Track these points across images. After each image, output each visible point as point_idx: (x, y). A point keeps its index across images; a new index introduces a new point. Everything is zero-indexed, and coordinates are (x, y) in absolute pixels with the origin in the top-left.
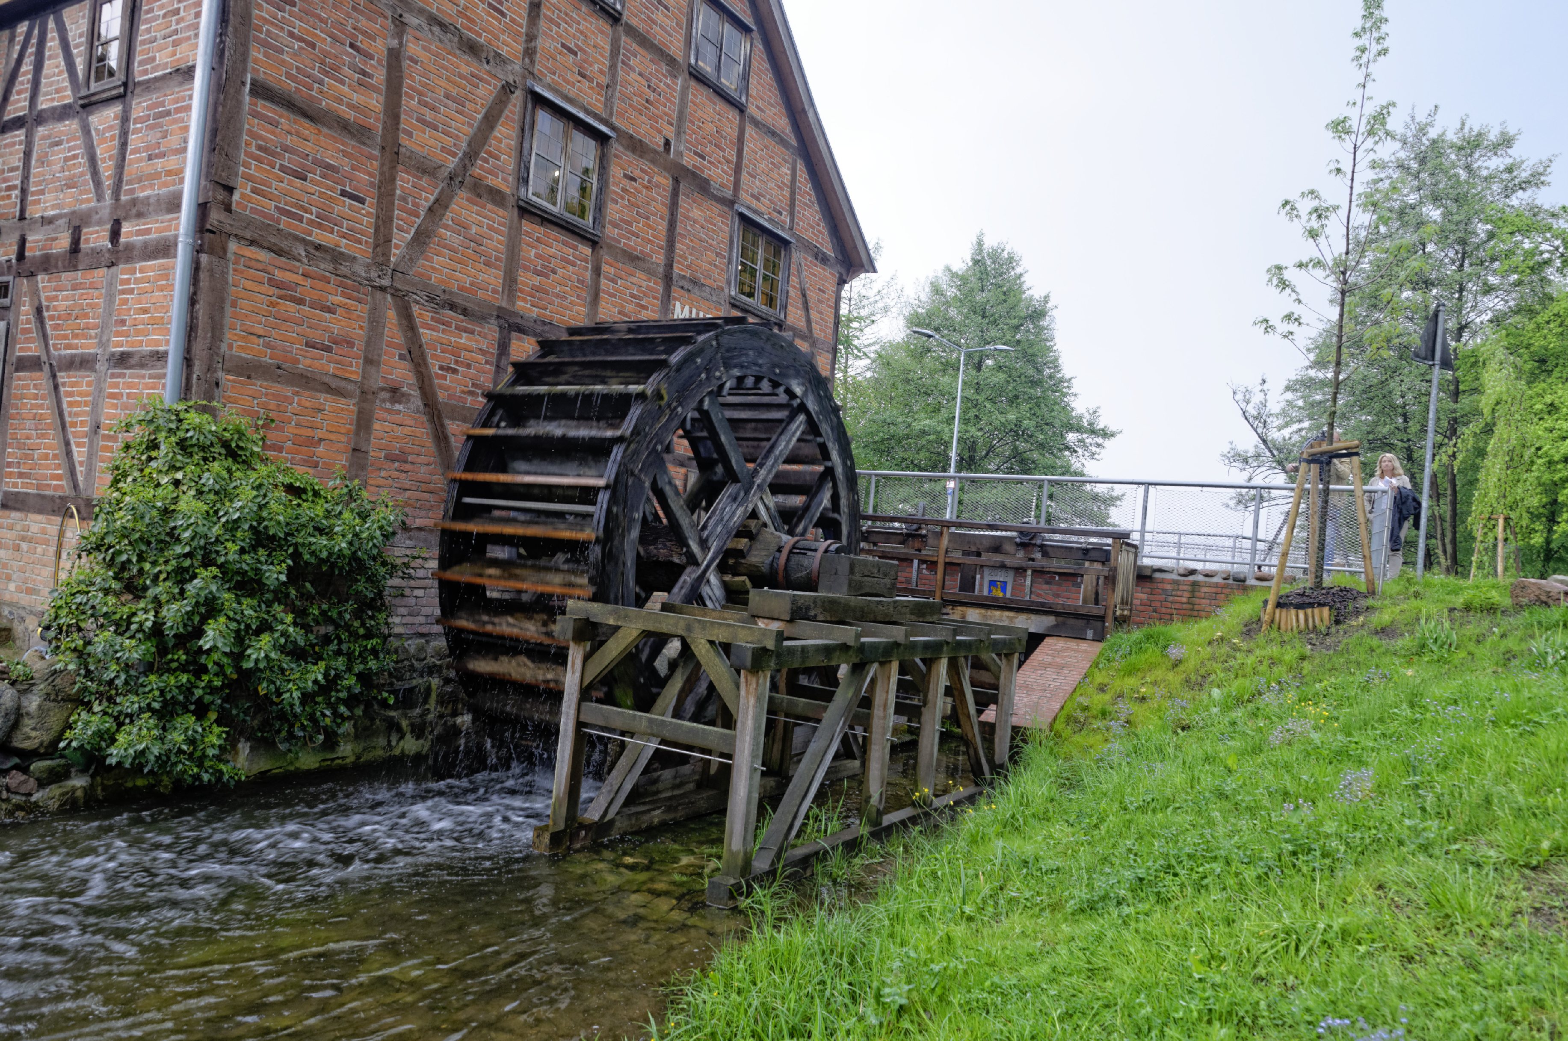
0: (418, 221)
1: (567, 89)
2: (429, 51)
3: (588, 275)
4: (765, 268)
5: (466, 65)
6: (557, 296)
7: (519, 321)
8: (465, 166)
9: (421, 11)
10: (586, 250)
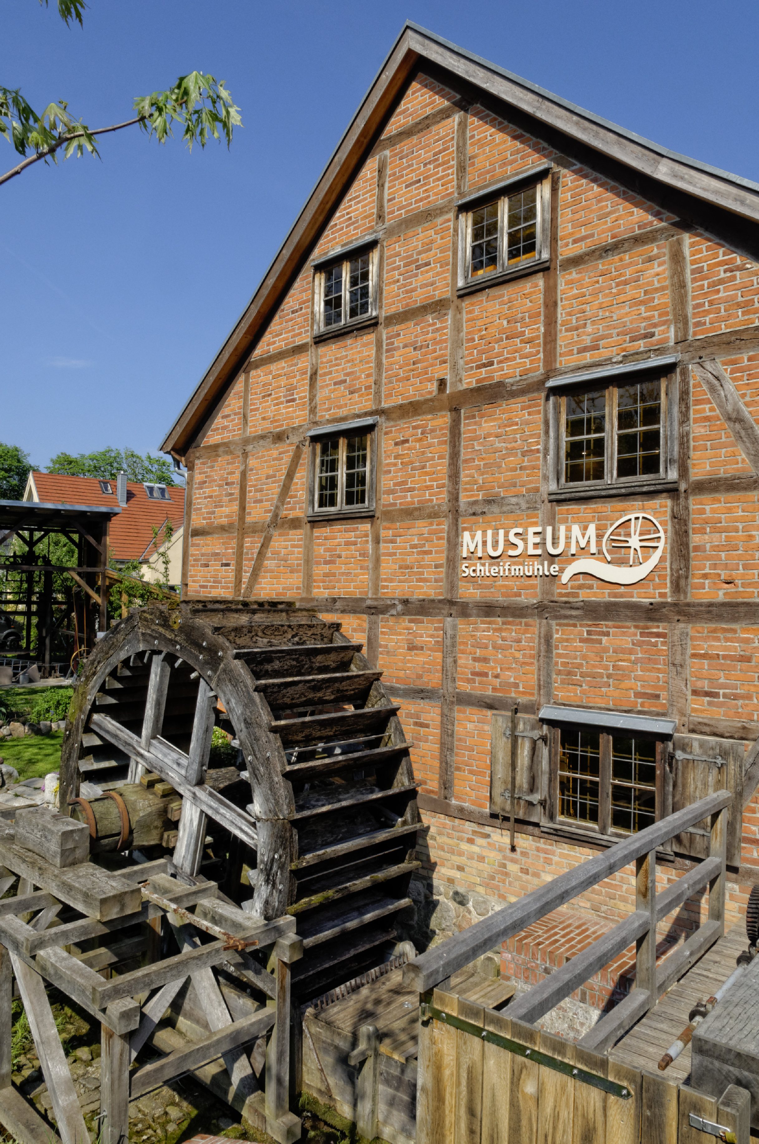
1: (342, 412)
3: (370, 546)
6: (343, 574)
9: (255, 438)
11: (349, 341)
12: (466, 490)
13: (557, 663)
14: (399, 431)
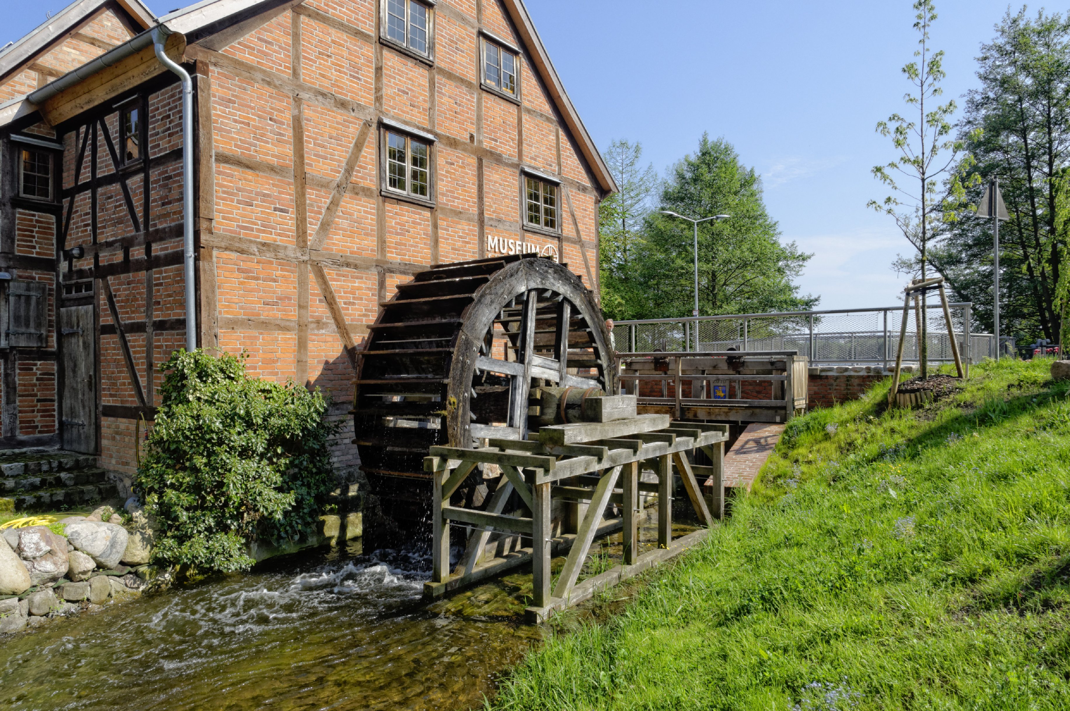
2: (317, 112)
4: (546, 202)
5: (340, 115)
6: (412, 246)
7: (389, 266)
8: (346, 178)
9: (310, 89)
10: (427, 214)
11: (410, 63)
14: (449, 154)
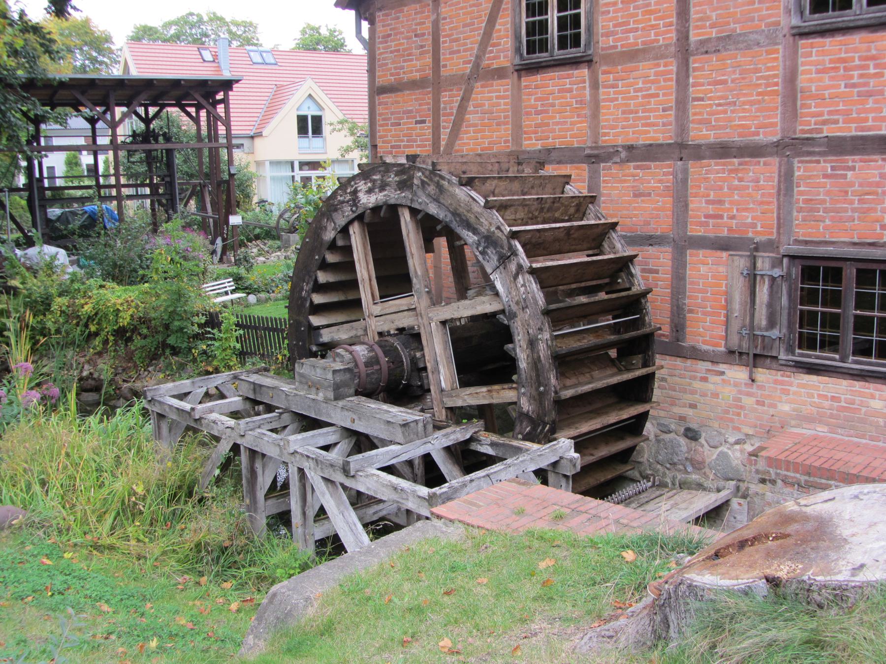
0: (453, 118)
6: (557, 123)
12: (697, 27)
13: (798, 200)
